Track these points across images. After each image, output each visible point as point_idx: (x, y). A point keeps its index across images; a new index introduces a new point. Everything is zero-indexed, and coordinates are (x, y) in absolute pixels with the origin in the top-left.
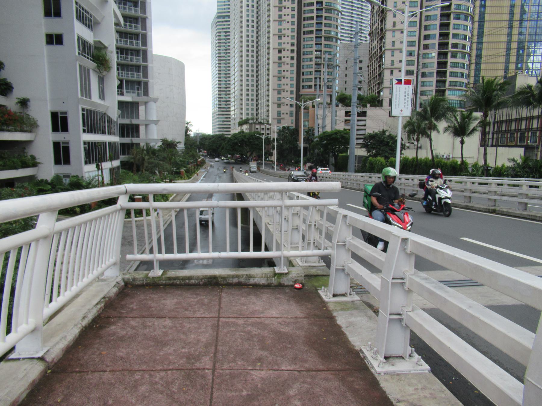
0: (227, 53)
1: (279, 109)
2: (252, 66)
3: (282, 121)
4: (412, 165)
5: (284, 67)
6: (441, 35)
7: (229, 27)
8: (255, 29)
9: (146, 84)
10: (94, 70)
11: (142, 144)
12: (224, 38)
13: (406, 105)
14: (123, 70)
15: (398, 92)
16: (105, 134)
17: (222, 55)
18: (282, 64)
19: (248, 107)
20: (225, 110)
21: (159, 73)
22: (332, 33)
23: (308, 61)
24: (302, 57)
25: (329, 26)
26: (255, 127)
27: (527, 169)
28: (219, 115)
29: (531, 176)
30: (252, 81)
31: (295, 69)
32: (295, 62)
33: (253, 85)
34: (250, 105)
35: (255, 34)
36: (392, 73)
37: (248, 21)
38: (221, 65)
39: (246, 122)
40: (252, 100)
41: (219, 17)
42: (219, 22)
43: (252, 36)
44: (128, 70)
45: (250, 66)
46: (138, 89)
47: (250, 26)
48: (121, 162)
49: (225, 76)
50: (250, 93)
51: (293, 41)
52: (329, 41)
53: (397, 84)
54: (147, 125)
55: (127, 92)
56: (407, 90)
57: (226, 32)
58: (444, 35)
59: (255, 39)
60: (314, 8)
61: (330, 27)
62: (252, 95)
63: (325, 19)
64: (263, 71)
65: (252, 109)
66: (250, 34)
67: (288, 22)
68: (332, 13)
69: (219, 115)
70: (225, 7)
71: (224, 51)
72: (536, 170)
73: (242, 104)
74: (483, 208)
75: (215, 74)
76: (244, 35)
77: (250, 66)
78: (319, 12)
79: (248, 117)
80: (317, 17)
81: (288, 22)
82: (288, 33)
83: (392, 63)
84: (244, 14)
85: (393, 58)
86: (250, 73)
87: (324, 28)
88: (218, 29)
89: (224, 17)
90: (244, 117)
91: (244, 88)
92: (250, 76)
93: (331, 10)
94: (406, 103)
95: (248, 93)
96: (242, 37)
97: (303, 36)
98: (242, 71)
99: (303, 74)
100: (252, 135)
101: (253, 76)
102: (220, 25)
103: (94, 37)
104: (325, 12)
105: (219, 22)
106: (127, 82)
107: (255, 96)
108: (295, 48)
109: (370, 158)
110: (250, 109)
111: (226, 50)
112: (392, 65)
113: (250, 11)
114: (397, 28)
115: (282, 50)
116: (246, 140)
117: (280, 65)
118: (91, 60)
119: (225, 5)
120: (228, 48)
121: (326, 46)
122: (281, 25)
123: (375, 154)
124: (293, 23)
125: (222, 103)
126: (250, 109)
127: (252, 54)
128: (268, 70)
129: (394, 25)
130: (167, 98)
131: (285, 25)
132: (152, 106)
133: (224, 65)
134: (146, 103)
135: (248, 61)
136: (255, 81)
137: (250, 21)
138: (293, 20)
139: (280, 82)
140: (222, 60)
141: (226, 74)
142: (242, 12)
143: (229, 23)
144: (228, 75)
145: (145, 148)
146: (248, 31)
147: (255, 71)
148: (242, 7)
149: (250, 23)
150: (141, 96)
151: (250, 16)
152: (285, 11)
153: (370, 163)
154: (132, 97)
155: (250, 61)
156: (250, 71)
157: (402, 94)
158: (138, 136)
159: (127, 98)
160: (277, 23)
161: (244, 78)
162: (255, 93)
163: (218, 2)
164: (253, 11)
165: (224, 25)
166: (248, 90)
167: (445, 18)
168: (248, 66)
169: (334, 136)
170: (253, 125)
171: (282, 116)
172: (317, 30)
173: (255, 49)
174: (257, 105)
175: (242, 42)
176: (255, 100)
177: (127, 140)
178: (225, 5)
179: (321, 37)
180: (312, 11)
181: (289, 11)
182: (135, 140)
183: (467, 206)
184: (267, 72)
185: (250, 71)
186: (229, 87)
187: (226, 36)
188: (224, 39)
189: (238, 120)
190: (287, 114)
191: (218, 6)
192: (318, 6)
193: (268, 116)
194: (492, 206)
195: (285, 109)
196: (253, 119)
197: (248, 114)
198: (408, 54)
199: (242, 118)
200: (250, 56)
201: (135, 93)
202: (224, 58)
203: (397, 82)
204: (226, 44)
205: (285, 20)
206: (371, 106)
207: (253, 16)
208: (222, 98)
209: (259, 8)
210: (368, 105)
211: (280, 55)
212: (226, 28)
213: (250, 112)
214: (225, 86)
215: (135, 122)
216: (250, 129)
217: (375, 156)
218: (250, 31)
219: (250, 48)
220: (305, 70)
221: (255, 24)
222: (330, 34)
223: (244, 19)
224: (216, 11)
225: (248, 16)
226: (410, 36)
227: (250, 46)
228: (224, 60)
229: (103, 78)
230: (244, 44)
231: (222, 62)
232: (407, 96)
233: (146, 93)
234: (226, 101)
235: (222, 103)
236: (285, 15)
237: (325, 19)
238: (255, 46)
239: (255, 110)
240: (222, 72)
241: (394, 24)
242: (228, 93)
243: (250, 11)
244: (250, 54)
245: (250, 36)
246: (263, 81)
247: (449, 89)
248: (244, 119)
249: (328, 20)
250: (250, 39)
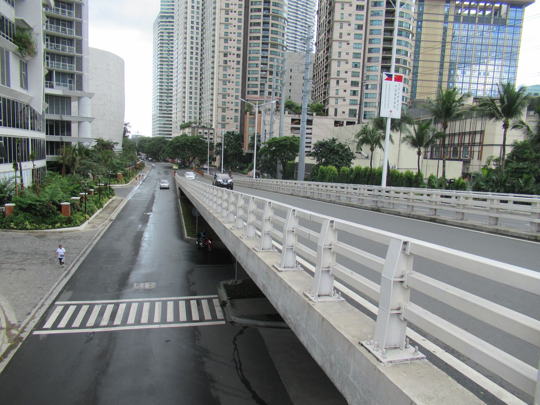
0: (169, 54)
1: (224, 114)
2: (196, 69)
3: (226, 125)
4: (365, 175)
5: (229, 71)
6: (384, 49)
7: (172, 28)
8: (200, 31)
9: (80, 77)
10: (14, 53)
11: (73, 144)
12: (167, 38)
13: (396, 105)
14: (53, 59)
15: (388, 90)
16: (28, 129)
17: (164, 56)
18: (228, 68)
19: (190, 110)
20: (166, 112)
21: (96, 68)
22: (279, 40)
23: (254, 67)
24: (248, 62)
25: (276, 33)
26: (198, 131)
27: (491, 183)
28: (160, 117)
29: (496, 190)
30: (196, 84)
31: (240, 73)
32: (241, 66)
33: (196, 89)
34: (193, 108)
35: (200, 37)
36: (338, 82)
37: (192, 22)
39: (188, 125)
40: (196, 103)
41: (162, 17)
42: (161, 22)
43: (197, 38)
44: (59, 60)
45: (194, 68)
46: (70, 82)
47: (195, 28)
48: (47, 162)
49: (167, 77)
52: (276, 48)
53: (386, 79)
54: (79, 123)
55: (57, 84)
56: (397, 88)
57: (169, 33)
58: (387, 50)
59: (199, 41)
60: (261, 14)
61: (277, 34)
62: (196, 98)
63: (272, 26)
64: (207, 74)
65: (195, 113)
66: (195, 36)
67: (235, 26)
68: (278, 21)
69: (160, 117)
70: (169, 7)
71: (167, 52)
72: (501, 185)
73: (184, 107)
74: (526, 235)
75: (156, 75)
76: (189, 36)
77: (194, 68)
78: (266, 18)
79: (190, 120)
80: (264, 23)
81: (235, 26)
82: (235, 37)
84: (189, 15)
85: (339, 69)
87: (270, 35)
88: (161, 29)
89: (167, 17)
90: (187, 121)
91: (187, 90)
92: (194, 78)
93: (278, 17)
94: (397, 103)
95: (191, 96)
96: (186, 38)
97: (249, 41)
98: (185, 73)
99: (249, 80)
100: (195, 139)
102: (163, 26)
103: (16, 15)
104: (272, 19)
105: (161, 22)
106: (58, 73)
107: (198, 99)
108: (241, 53)
109: (321, 167)
110: (193, 113)
111: (169, 51)
112: (338, 75)
113: (195, 13)
114: (343, 39)
115: (228, 54)
116: (188, 143)
117: (225, 69)
118: (11, 40)
119: (168, 5)
120: (171, 49)
121: (272, 53)
122: (227, 28)
123: (324, 163)
124: (239, 28)
125: (163, 105)
126: (193, 113)
127: (197, 56)
128: (213, 73)
129: (341, 37)
130: (104, 95)
131: (231, 29)
132: (86, 101)
133: (167, 67)
134: (79, 98)
135: (191, 63)
136: (199, 84)
137: (195, 23)
138: (240, 24)
139: (225, 86)
140: (164, 61)
141: (168, 76)
142: (186, 13)
143: (172, 24)
144: (170, 77)
145: (77, 147)
146: (192, 32)
148: (186, 8)
149: (195, 25)
150: (74, 90)
151: (195, 18)
152: (231, 15)
153: (321, 171)
154: (63, 91)
155: (194, 63)
156: (194, 73)
157: (392, 93)
158: (69, 134)
159: (57, 91)
160: (223, 26)
161: (188, 80)
162: (198, 96)
163: (162, 2)
164: (198, 13)
165: (167, 26)
166: (191, 93)
167: (389, 34)
168: (191, 68)
169: (283, 143)
170: (196, 129)
171: (227, 121)
172: (263, 37)
173: (199, 52)
175: (186, 43)
176: (198, 104)
177: (55, 138)
178: (168, 5)
179: (267, 44)
180: (259, 17)
181: (236, 15)
182: (66, 139)
183: (498, 230)
184: (211, 76)
185: (194, 73)
186: (172, 90)
187: (169, 37)
188: (167, 40)
189: (180, 123)
190: (231, 119)
191: (161, 5)
192: (265, 12)
193: (211, 121)
194: (433, 215)
195: (230, 114)
196: (195, 123)
197: (190, 117)
198: (354, 66)
199: (184, 122)
200: (194, 58)
201: (67, 86)
202: (167, 60)
203: (387, 77)
204: (169, 45)
205: (231, 24)
206: (317, 115)
207: (198, 18)
208: (164, 100)
209: (205, 10)
210: (315, 114)
211: (225, 59)
212: (169, 29)
213: (193, 115)
214: (166, 88)
215: (66, 118)
216: (193, 132)
217: (325, 164)
218: (195, 33)
220: (251, 76)
222: (276, 41)
223: (189, 20)
224: (159, 10)
225: (193, 17)
226: (356, 48)
227: (194, 48)
228: (167, 61)
229: (26, 64)
230: (188, 46)
231: (164, 63)
232: (397, 95)
233: (80, 87)
234: (168, 104)
235: (163, 105)
236: (231, 19)
238: (200, 49)
239: (198, 114)
240: (163, 74)
242: (170, 95)
243: (195, 13)
244: (194, 56)
245: (195, 38)
246: (207, 84)
248: (186, 122)
249: (275, 27)
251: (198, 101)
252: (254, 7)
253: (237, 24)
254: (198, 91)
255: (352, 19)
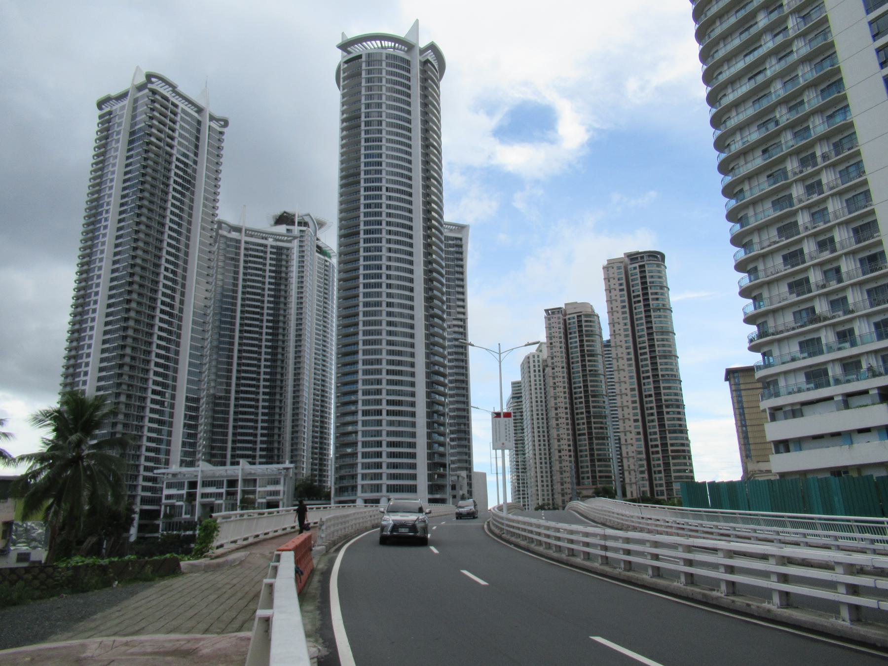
2: (545, 454)
8: (545, 421)
24: (579, 454)
32: (572, 459)
33: (546, 472)
35: (545, 425)
37: (538, 415)
38: (519, 446)
40: (547, 486)
41: (513, 398)
50: (544, 479)
51: (569, 443)
59: (545, 429)
62: (547, 481)
66: (541, 425)
76: (536, 426)
83: (629, 466)
84: (534, 409)
86: (543, 461)
101: (546, 463)
108: (572, 448)
117: (560, 463)
131: (562, 431)
135: (540, 450)
136: (548, 468)
147: (548, 458)
149: (540, 416)
152: (560, 421)
155: (542, 449)
156: (543, 458)
161: (538, 465)
162: (549, 479)
166: (542, 477)
168: (540, 454)
173: (546, 438)
174: (552, 491)
175: (534, 432)
176: (550, 486)
180: (583, 418)
181: (564, 420)
185: (543, 458)
197: (544, 500)
207: (542, 410)
213: (546, 498)
219: (542, 438)
221: (544, 416)
223: (535, 413)
225: (537, 410)
230: (536, 434)
237: (594, 423)
239: (550, 495)
241: (626, 440)
247: (676, 482)
250: (541, 430)
251: (549, 483)
252: (579, 411)
253: (566, 427)
254: (549, 474)
255: (632, 429)
